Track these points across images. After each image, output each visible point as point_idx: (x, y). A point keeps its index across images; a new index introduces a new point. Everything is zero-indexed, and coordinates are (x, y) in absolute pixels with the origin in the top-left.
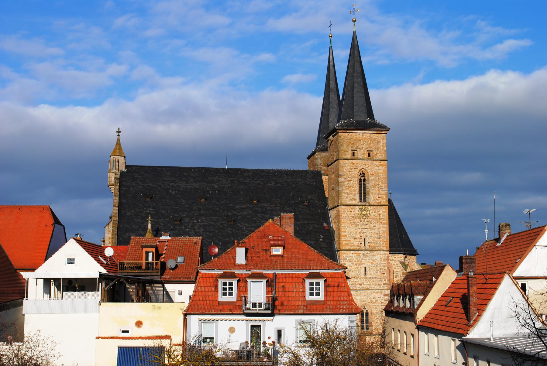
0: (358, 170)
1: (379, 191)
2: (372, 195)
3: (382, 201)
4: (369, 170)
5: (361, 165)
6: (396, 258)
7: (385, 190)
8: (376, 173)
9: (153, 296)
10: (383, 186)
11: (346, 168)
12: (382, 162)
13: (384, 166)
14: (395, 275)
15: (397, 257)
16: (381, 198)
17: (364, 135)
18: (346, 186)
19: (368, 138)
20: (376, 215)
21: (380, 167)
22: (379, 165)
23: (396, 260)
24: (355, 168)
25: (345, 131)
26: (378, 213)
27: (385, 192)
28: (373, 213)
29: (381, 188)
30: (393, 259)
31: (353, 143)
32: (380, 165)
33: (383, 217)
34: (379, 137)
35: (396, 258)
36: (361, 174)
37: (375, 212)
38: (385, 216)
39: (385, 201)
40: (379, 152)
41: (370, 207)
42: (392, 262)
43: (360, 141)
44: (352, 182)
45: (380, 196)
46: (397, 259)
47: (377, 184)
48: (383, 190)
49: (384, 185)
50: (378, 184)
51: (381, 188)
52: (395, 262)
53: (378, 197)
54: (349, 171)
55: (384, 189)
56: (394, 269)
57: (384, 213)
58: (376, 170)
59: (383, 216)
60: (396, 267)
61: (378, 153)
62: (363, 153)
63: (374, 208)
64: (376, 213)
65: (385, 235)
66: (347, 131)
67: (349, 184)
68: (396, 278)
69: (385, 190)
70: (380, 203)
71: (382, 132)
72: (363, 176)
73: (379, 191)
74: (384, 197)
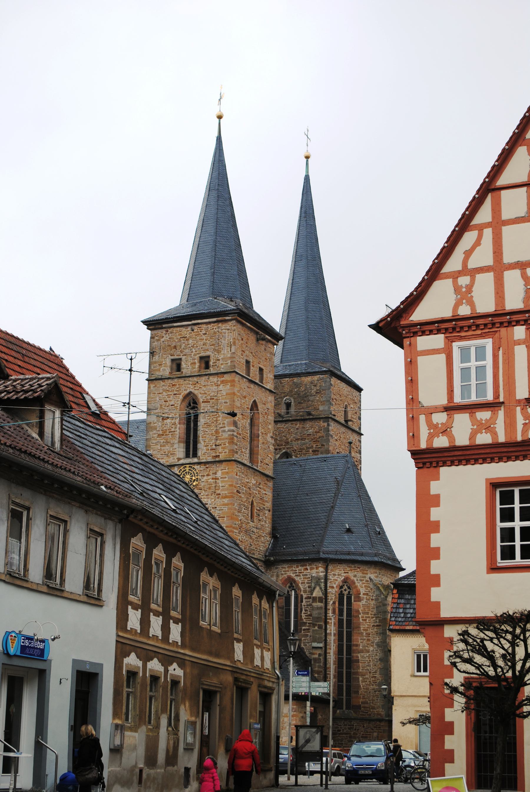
0: (181, 397)
1: (217, 432)
2: (205, 442)
3: (222, 453)
4: (200, 393)
5: (187, 387)
6: (307, 569)
7: (229, 431)
8: (213, 399)
9: (270, 691)
10: (225, 422)
11: (160, 395)
12: (225, 375)
13: (229, 384)
14: (304, 606)
15: (308, 568)
16: (220, 447)
17: (195, 328)
18: (159, 431)
19: (201, 333)
20: (211, 480)
21: (221, 386)
22: (219, 383)
23: (306, 575)
24: (175, 392)
25: (160, 326)
26: (214, 476)
27: (229, 433)
28: (205, 478)
29: (222, 428)
30: (301, 573)
31: (175, 347)
32: (222, 382)
33: (223, 484)
34: (223, 328)
35: (307, 569)
36: (190, 404)
37: (208, 475)
38: (227, 481)
39: (227, 451)
40: (220, 358)
41: (199, 467)
42: (299, 578)
43: (187, 340)
44: (169, 421)
45: (218, 442)
46: (309, 571)
47: (215, 419)
48: (224, 431)
49: (227, 420)
50: (217, 421)
51: (222, 428)
52: (306, 578)
53: (216, 445)
54: (165, 401)
55: (227, 429)
56: (302, 593)
57: (225, 476)
58: (214, 392)
59: (222, 482)
60: (307, 589)
61: (219, 360)
62: (192, 364)
63: (207, 468)
64: (209, 477)
65: (225, 519)
66: (164, 326)
67: (163, 426)
68: (306, 610)
69: (229, 431)
70: (219, 456)
71: (227, 318)
72: (193, 408)
73: (217, 432)
74: (227, 443)
